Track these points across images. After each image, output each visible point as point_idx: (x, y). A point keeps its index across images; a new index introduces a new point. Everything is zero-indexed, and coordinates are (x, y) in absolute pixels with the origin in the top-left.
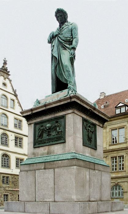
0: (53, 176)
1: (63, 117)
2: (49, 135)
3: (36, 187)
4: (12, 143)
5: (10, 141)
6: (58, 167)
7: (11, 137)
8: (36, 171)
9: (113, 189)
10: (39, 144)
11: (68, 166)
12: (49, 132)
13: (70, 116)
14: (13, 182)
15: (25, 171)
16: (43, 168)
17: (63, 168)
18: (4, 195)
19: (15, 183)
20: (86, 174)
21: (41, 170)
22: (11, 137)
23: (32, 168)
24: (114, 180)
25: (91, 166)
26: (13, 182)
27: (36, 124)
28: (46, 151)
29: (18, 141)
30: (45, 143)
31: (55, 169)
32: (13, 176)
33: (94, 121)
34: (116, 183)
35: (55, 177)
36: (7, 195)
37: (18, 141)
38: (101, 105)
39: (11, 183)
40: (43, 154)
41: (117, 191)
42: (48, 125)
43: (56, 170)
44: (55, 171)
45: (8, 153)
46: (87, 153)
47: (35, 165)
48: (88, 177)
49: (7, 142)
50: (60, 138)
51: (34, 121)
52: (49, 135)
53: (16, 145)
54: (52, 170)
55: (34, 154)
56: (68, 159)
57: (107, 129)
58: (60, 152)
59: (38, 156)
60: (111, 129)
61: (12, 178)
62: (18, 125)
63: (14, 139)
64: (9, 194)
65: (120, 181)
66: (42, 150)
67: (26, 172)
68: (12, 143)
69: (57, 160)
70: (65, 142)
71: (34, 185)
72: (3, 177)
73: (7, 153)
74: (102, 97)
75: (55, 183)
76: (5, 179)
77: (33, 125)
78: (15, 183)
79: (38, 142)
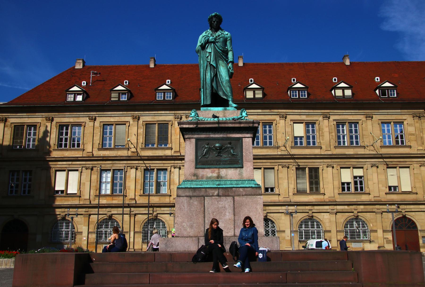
0: (232, 205)
1: (240, 140)
2: (220, 156)
3: (206, 219)
6: (239, 195)
8: (206, 197)
10: (202, 165)
11: (252, 195)
12: (219, 153)
13: (247, 140)
15: (187, 196)
16: (216, 194)
17: (246, 196)
21: (214, 197)
23: (197, 193)
27: (197, 140)
28: (215, 175)
30: (212, 164)
31: (235, 197)
35: (236, 207)
40: (210, 178)
42: (217, 145)
44: (235, 199)
47: (204, 190)
50: (236, 162)
51: (196, 136)
52: (220, 156)
54: (230, 199)
55: (195, 175)
56: (251, 187)
59: (202, 179)
65: (116, 212)
66: (208, 173)
67: (188, 199)
69: (237, 187)
70: (242, 167)
71: (203, 215)
75: (236, 214)
77: (194, 141)
79: (201, 162)
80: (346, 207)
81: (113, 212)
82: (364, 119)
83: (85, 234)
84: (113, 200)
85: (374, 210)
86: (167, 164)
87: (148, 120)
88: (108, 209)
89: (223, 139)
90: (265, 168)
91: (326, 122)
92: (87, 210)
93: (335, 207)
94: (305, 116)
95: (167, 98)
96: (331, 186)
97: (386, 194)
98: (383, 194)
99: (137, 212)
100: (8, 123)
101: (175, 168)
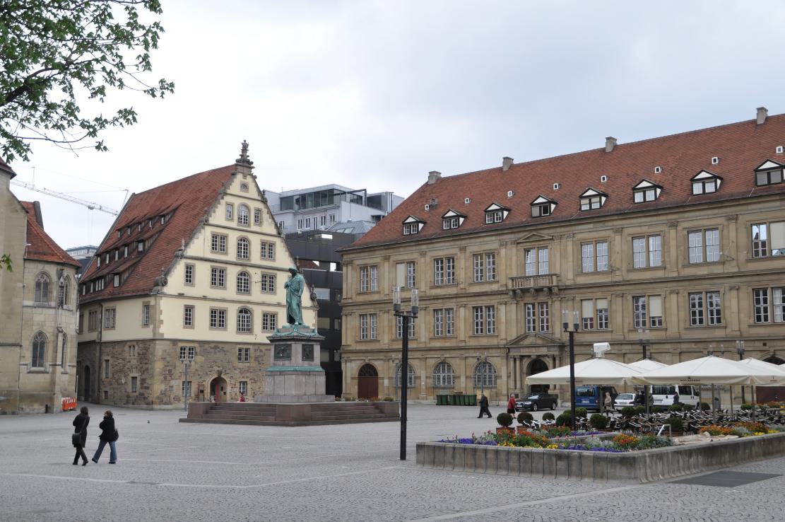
1: (291, 345)
4: (256, 288)
5: (253, 284)
7: (256, 275)
9: (439, 369)
14: (256, 358)
18: (240, 382)
19: (260, 359)
20: (303, 379)
22: (256, 275)
24: (438, 352)
25: (307, 373)
26: (256, 358)
29: (268, 283)
32: (256, 347)
33: (311, 343)
34: (442, 359)
36: (245, 383)
37: (268, 283)
38: (427, 202)
39: (253, 360)
41: (446, 374)
43: (286, 376)
45: (250, 306)
46: (306, 365)
48: (304, 380)
49: (247, 287)
50: (289, 357)
53: (264, 289)
57: (427, 258)
58: (289, 365)
60: (433, 258)
61: (256, 350)
62: (268, 250)
63: (260, 279)
64: (248, 380)
68: (256, 288)
72: (240, 350)
73: (248, 305)
74: (433, 182)
76: (243, 353)
78: (260, 359)
80: (693, 345)
81: (446, 356)
82: (726, 223)
83: (423, 378)
84: (445, 342)
85: (730, 349)
86: (493, 301)
87: (475, 250)
88: (442, 352)
89: (284, 345)
90: (596, 299)
91: (673, 232)
92: (424, 353)
93: (679, 345)
94: (647, 227)
95: (497, 220)
96: (675, 319)
97: (750, 326)
98: (744, 327)
99: (467, 355)
100: (354, 266)
101: (501, 304)
